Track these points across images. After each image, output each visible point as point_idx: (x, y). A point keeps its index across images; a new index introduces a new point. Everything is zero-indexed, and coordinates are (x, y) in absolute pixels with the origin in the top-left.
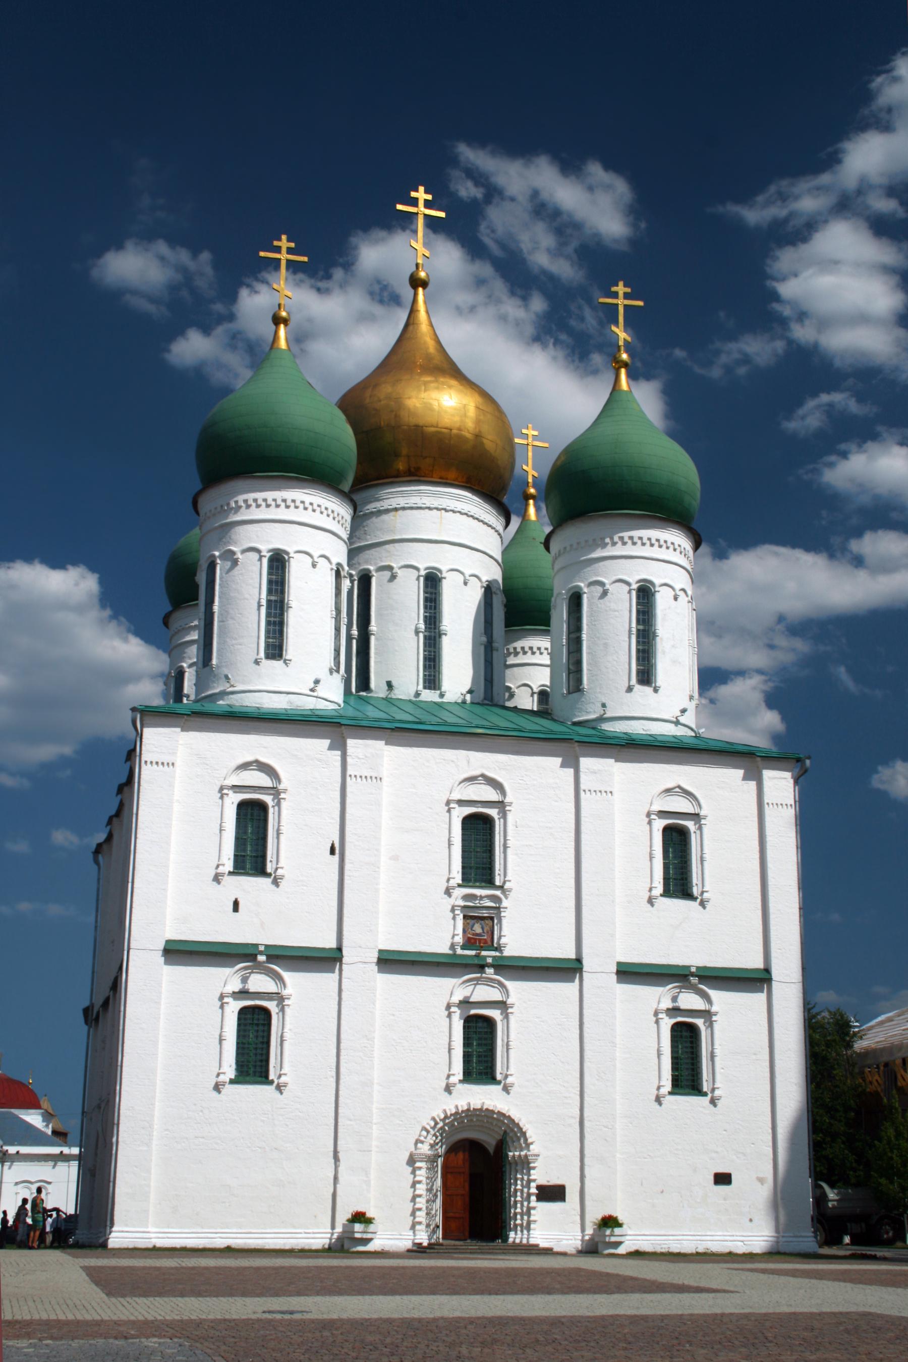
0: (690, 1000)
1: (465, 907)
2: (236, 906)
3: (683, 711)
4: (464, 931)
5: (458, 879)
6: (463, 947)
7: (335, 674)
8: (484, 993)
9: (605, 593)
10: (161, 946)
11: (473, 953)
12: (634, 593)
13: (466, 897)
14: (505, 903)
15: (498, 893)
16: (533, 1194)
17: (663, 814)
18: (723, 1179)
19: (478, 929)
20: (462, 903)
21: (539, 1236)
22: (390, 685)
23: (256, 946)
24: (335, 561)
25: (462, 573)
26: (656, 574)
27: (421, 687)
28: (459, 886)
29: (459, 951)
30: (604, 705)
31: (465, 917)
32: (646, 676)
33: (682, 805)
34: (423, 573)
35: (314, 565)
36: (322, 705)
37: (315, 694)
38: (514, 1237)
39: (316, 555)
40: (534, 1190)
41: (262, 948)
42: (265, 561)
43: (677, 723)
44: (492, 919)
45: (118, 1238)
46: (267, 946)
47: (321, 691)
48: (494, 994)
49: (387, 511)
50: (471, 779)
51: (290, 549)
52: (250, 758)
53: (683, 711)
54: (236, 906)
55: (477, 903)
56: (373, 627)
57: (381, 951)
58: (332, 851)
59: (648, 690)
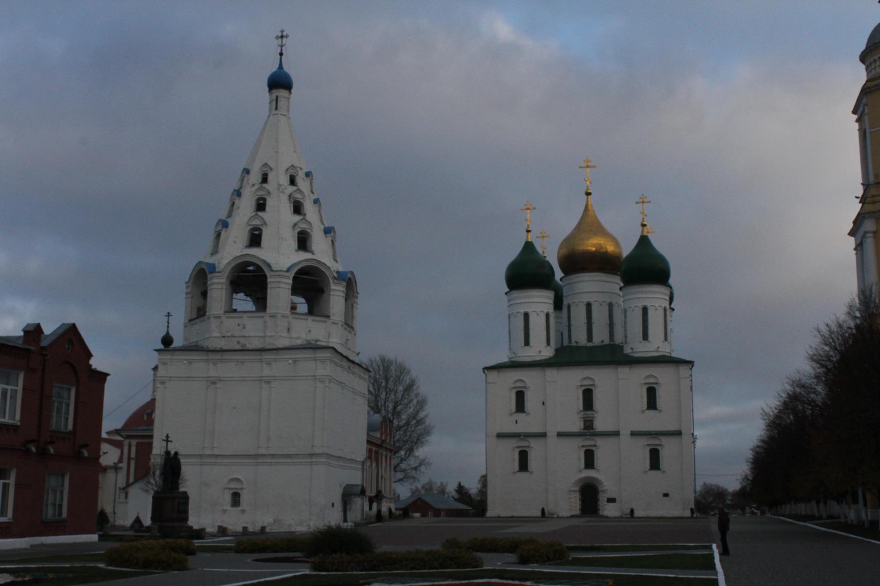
0: (656, 442)
1: (583, 418)
2: (516, 422)
3: (658, 348)
4: (584, 425)
5: (582, 409)
6: (584, 429)
7: (549, 347)
8: (587, 443)
9: (633, 310)
10: (495, 434)
11: (587, 431)
12: (641, 311)
13: (585, 414)
14: (596, 415)
15: (593, 412)
16: (605, 501)
17: (646, 384)
18: (666, 495)
19: (589, 424)
20: (583, 416)
21: (606, 513)
22: (576, 342)
23: (521, 433)
24: (546, 311)
25: (598, 301)
26: (648, 304)
27: (586, 342)
28: (582, 411)
29: (582, 431)
30: (632, 349)
31: (584, 420)
32: (645, 337)
33: (652, 380)
34: (585, 303)
35: (538, 314)
36: (543, 358)
37: (540, 355)
38: (601, 513)
39: (538, 311)
40: (606, 500)
41: (522, 434)
42: (522, 316)
43: (657, 351)
44: (592, 420)
45: (490, 513)
46: (524, 433)
47: (542, 354)
48: (592, 443)
49: (576, 282)
50: (585, 378)
51: (529, 310)
52: (517, 379)
53: (658, 348)
54: (516, 422)
55: (587, 416)
56: (572, 322)
57: (558, 433)
58: (543, 404)
59: (645, 342)
